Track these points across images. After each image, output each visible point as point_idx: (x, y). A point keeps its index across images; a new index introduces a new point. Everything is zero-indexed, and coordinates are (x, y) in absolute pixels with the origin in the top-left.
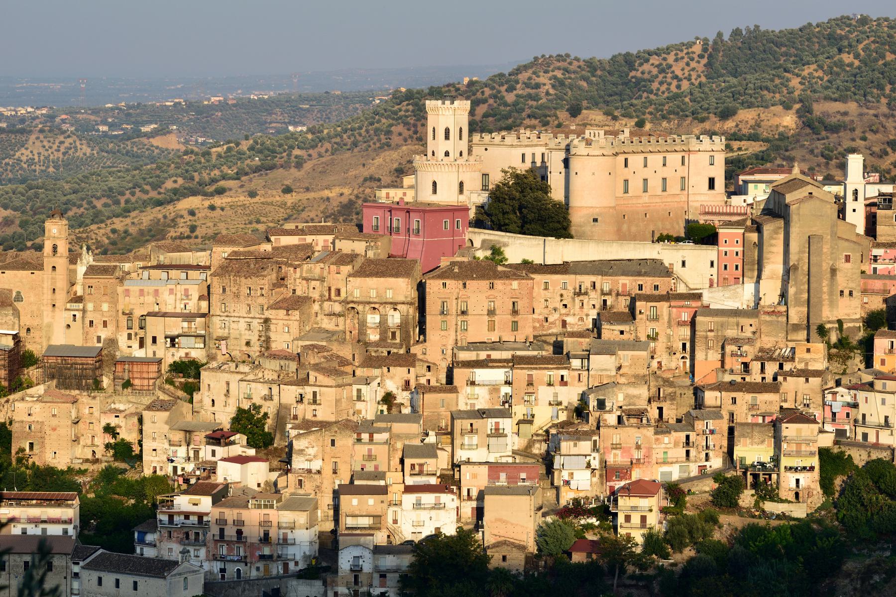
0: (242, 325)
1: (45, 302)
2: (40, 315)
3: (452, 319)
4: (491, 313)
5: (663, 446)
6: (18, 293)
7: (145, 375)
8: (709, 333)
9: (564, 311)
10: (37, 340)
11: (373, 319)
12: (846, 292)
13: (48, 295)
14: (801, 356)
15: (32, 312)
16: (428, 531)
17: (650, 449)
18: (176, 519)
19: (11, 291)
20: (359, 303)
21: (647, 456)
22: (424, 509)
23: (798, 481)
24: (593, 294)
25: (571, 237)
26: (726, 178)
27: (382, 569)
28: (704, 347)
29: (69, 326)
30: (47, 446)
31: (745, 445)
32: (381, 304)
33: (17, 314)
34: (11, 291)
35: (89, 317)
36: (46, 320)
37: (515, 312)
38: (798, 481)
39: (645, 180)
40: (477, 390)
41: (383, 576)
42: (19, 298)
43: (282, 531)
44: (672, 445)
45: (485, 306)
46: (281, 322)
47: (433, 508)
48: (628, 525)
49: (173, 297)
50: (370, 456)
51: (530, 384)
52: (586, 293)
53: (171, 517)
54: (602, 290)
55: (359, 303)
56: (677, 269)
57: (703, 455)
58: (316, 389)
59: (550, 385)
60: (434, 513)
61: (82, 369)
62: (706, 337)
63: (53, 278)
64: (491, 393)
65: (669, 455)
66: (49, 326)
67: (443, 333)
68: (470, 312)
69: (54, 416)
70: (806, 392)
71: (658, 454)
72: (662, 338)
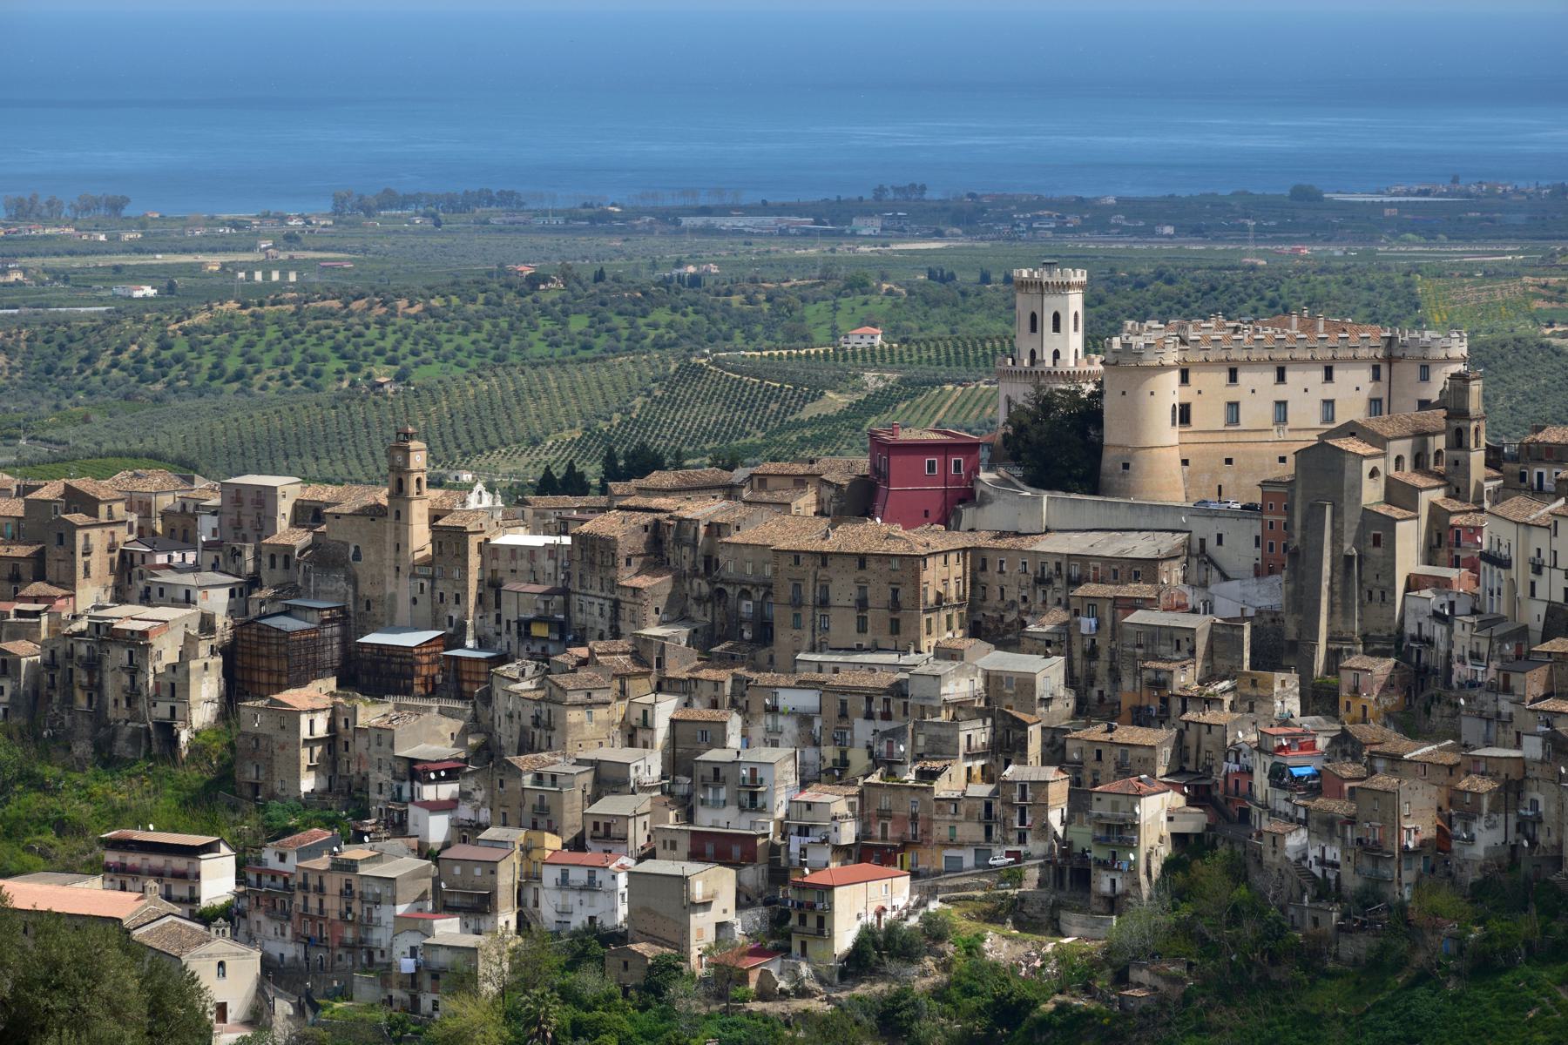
0: (596, 610)
1: (387, 563)
2: (382, 583)
3: (807, 614)
4: (862, 604)
5: (948, 817)
6: (357, 548)
7: (473, 677)
8: (1139, 651)
9: (1023, 607)
10: (379, 617)
11: (746, 607)
12: (1377, 594)
13: (389, 554)
14: (1244, 691)
15: (373, 576)
16: (578, 921)
17: (930, 820)
18: (266, 880)
19: (292, 548)
20: (728, 583)
21: (927, 832)
22: (572, 889)
23: (1113, 881)
24: (1058, 584)
25: (1095, 491)
26: (1100, 412)
27: (434, 967)
28: (1130, 671)
29: (414, 601)
30: (276, 771)
31: (1081, 824)
32: (754, 585)
33: (353, 580)
34: (347, 545)
35: (440, 584)
36: (389, 589)
37: (895, 605)
38: (1113, 881)
39: (1281, 405)
40: (781, 721)
41: (435, 976)
42: (357, 556)
43: (367, 906)
44: (962, 817)
45: (855, 591)
46: (628, 606)
47: (582, 889)
48: (801, 929)
49: (552, 562)
50: (542, 807)
51: (843, 715)
52: (1049, 581)
53: (259, 877)
54: (1069, 576)
55: (728, 583)
56: (1211, 544)
57: (1014, 836)
58: (552, 707)
59: (869, 716)
60: (585, 896)
61: (401, 664)
62: (1134, 656)
63: (397, 528)
64: (800, 725)
65: (959, 831)
66: (393, 597)
67: (795, 632)
68: (833, 601)
69: (283, 728)
70: (1210, 747)
71: (941, 831)
72: (1104, 655)
